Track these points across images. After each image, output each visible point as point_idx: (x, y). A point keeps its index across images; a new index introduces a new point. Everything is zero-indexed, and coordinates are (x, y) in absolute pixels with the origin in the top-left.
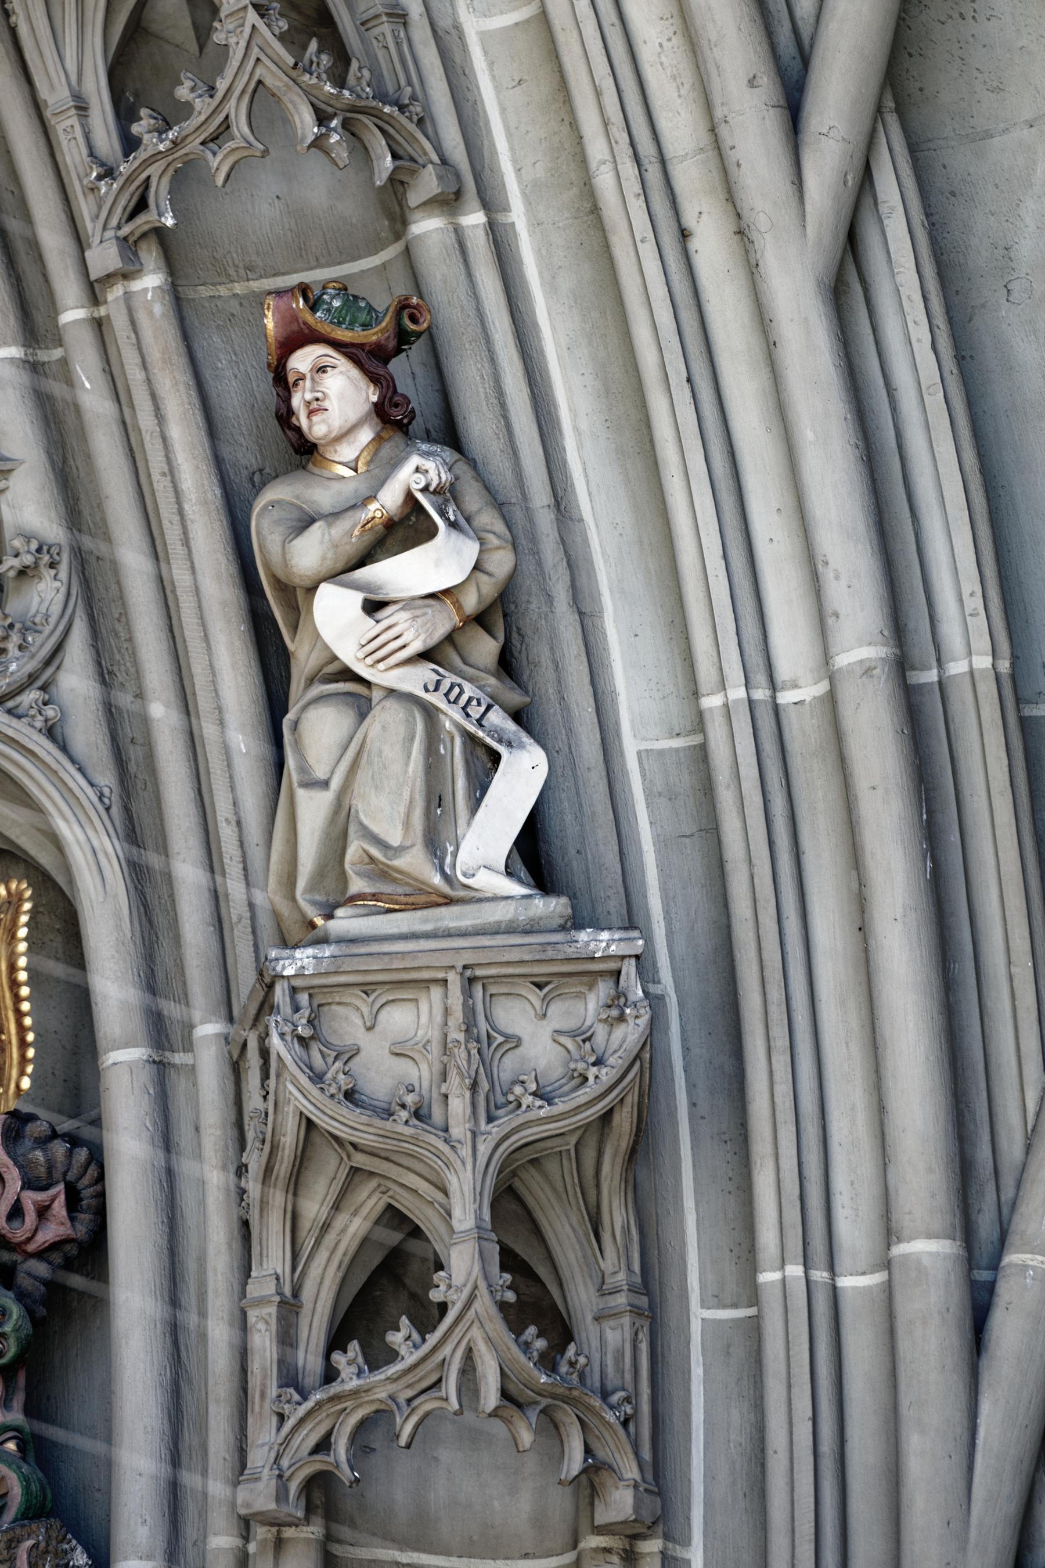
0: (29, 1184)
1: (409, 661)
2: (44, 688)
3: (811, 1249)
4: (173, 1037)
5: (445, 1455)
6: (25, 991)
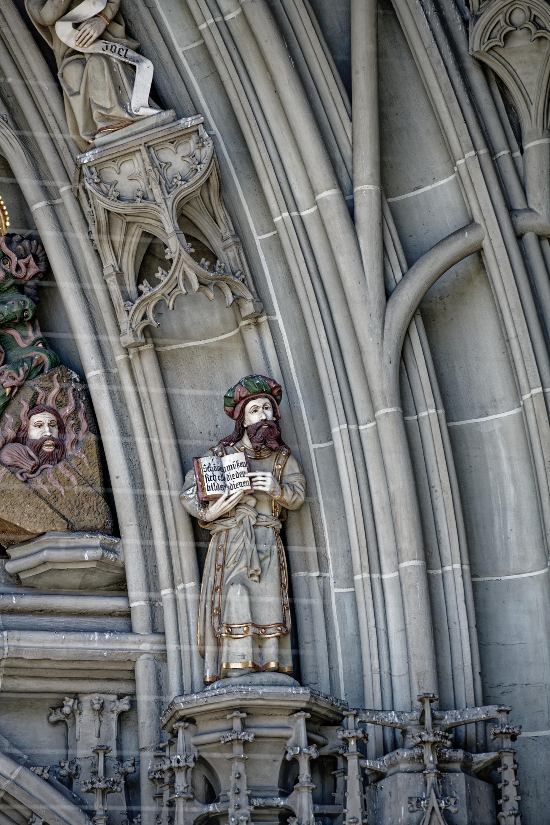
0: (20, 257)
1: (94, 41)
3: (289, 205)
4: (53, 195)
5: (186, 309)
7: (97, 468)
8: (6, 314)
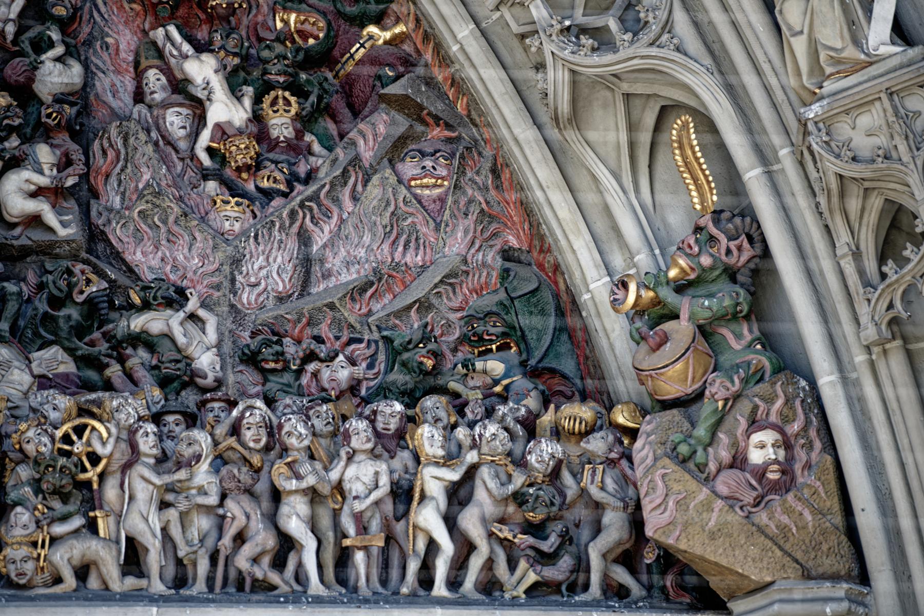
2: (669, 32)
6: (702, 160)
7: (836, 499)
8: (715, 309)
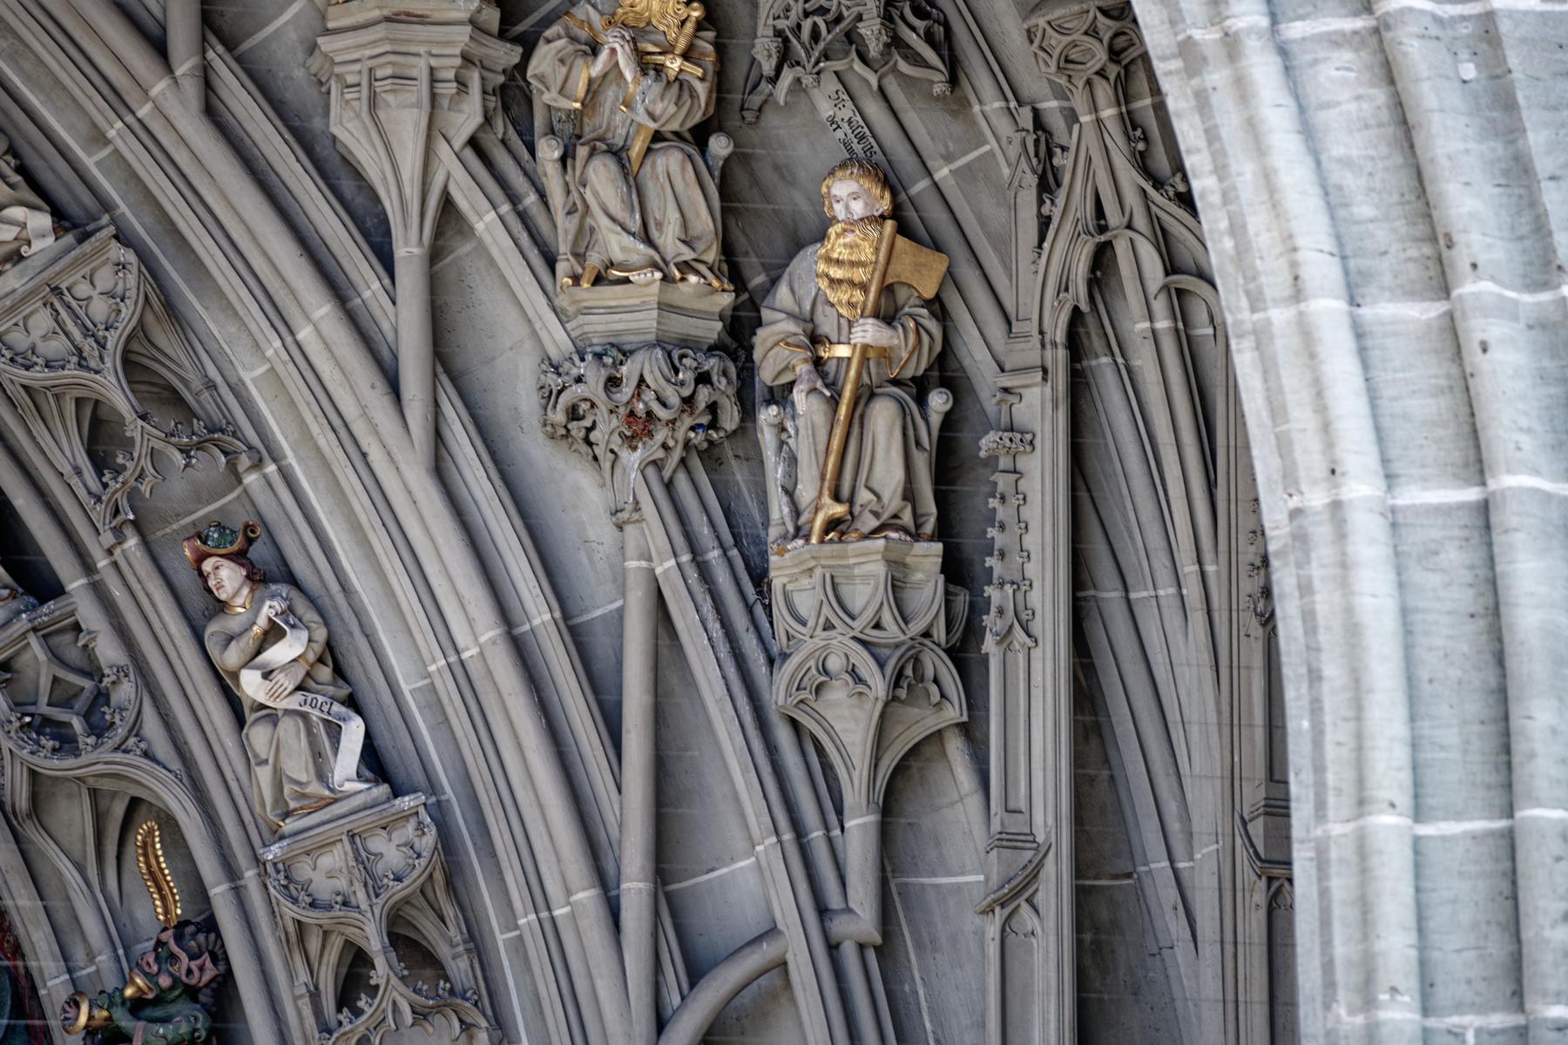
0: (192, 957)
1: (291, 694)
2: (136, 735)
6: (166, 872)
